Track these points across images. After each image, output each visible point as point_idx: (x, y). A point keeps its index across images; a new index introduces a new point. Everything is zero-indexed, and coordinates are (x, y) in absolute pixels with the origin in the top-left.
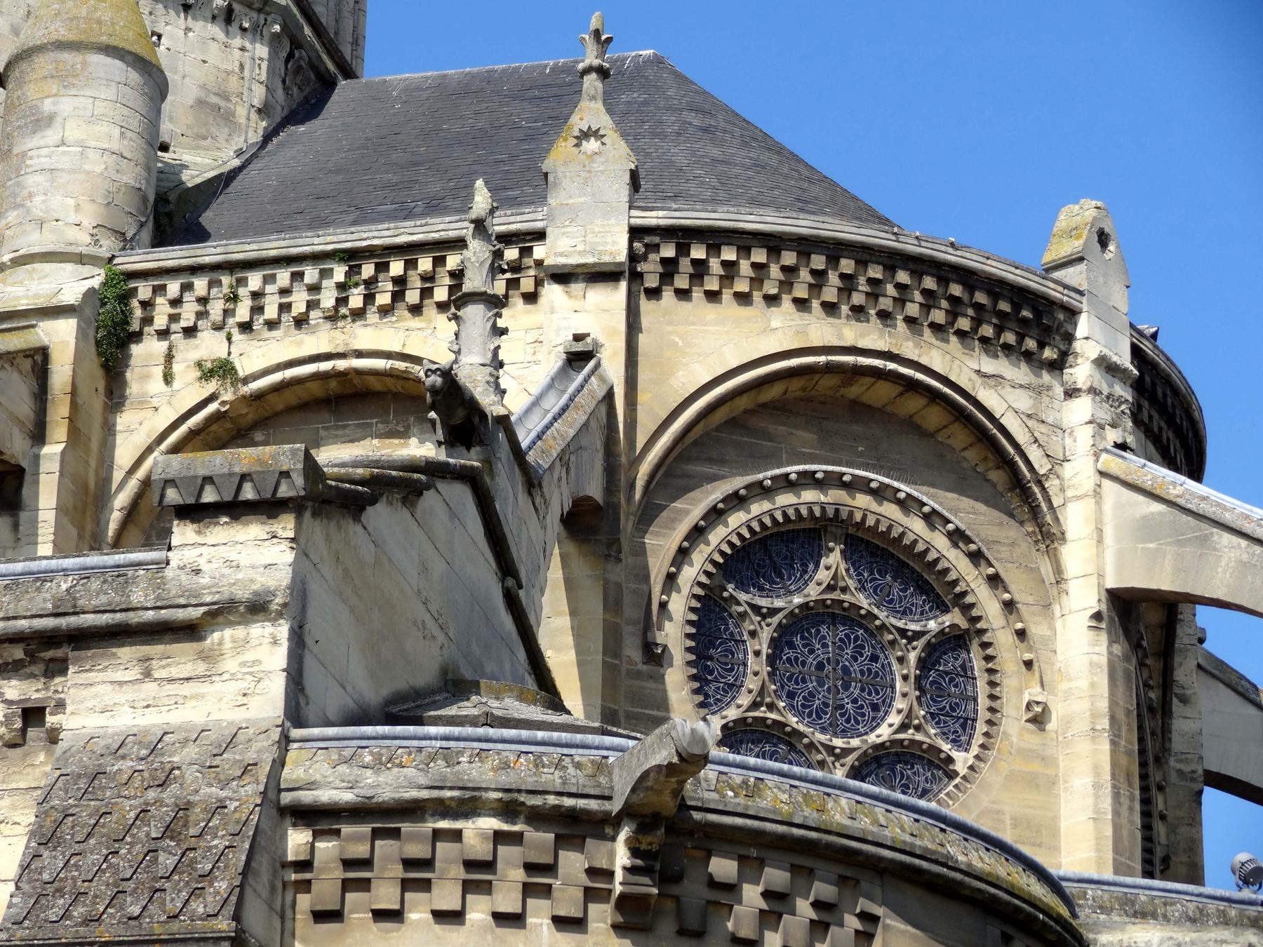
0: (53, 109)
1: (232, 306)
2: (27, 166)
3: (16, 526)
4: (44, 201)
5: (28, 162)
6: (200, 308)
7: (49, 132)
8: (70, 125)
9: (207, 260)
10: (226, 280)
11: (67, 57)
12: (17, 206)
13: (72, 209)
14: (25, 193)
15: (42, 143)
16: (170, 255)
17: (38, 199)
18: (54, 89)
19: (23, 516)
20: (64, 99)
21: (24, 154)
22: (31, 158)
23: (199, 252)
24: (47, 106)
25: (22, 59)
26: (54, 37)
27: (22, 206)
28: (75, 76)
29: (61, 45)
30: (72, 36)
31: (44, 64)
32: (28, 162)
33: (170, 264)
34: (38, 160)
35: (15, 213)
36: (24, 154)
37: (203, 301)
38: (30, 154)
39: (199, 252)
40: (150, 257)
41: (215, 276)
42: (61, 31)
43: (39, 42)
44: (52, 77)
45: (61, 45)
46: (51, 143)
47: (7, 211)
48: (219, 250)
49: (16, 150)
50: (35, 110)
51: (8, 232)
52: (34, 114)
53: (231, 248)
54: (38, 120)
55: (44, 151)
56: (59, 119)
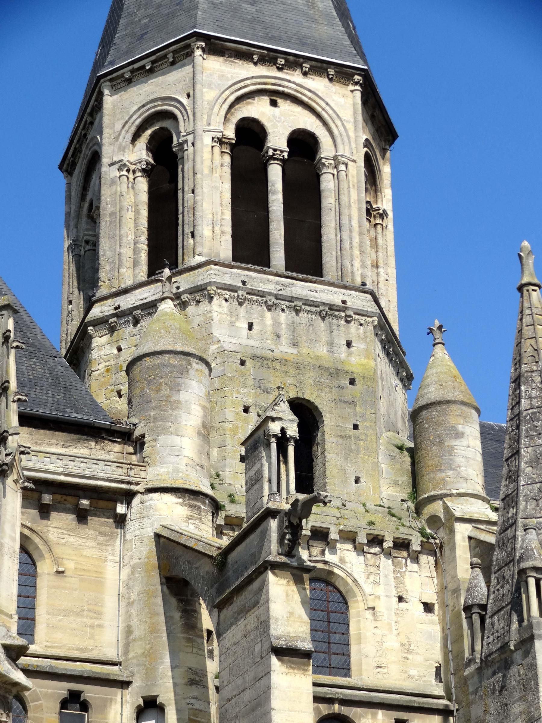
0: (463, 430)
2: (455, 453)
4: (466, 470)
5: (455, 451)
7: (462, 440)
8: (470, 439)
11: (464, 408)
12: (451, 469)
13: (476, 476)
15: (460, 444)
17: (463, 469)
18: (462, 422)
20: (466, 427)
21: (452, 447)
22: (456, 449)
24: (460, 428)
26: (460, 399)
27: (456, 470)
28: (469, 418)
29: (463, 403)
30: (465, 400)
31: (456, 409)
32: (455, 451)
34: (460, 451)
35: (451, 472)
36: (452, 447)
38: (456, 447)
42: (461, 397)
43: (453, 399)
45: (463, 403)
47: (445, 469)
49: (446, 444)
50: (454, 429)
52: (455, 431)
54: (457, 433)
55: (462, 448)
56: (466, 435)
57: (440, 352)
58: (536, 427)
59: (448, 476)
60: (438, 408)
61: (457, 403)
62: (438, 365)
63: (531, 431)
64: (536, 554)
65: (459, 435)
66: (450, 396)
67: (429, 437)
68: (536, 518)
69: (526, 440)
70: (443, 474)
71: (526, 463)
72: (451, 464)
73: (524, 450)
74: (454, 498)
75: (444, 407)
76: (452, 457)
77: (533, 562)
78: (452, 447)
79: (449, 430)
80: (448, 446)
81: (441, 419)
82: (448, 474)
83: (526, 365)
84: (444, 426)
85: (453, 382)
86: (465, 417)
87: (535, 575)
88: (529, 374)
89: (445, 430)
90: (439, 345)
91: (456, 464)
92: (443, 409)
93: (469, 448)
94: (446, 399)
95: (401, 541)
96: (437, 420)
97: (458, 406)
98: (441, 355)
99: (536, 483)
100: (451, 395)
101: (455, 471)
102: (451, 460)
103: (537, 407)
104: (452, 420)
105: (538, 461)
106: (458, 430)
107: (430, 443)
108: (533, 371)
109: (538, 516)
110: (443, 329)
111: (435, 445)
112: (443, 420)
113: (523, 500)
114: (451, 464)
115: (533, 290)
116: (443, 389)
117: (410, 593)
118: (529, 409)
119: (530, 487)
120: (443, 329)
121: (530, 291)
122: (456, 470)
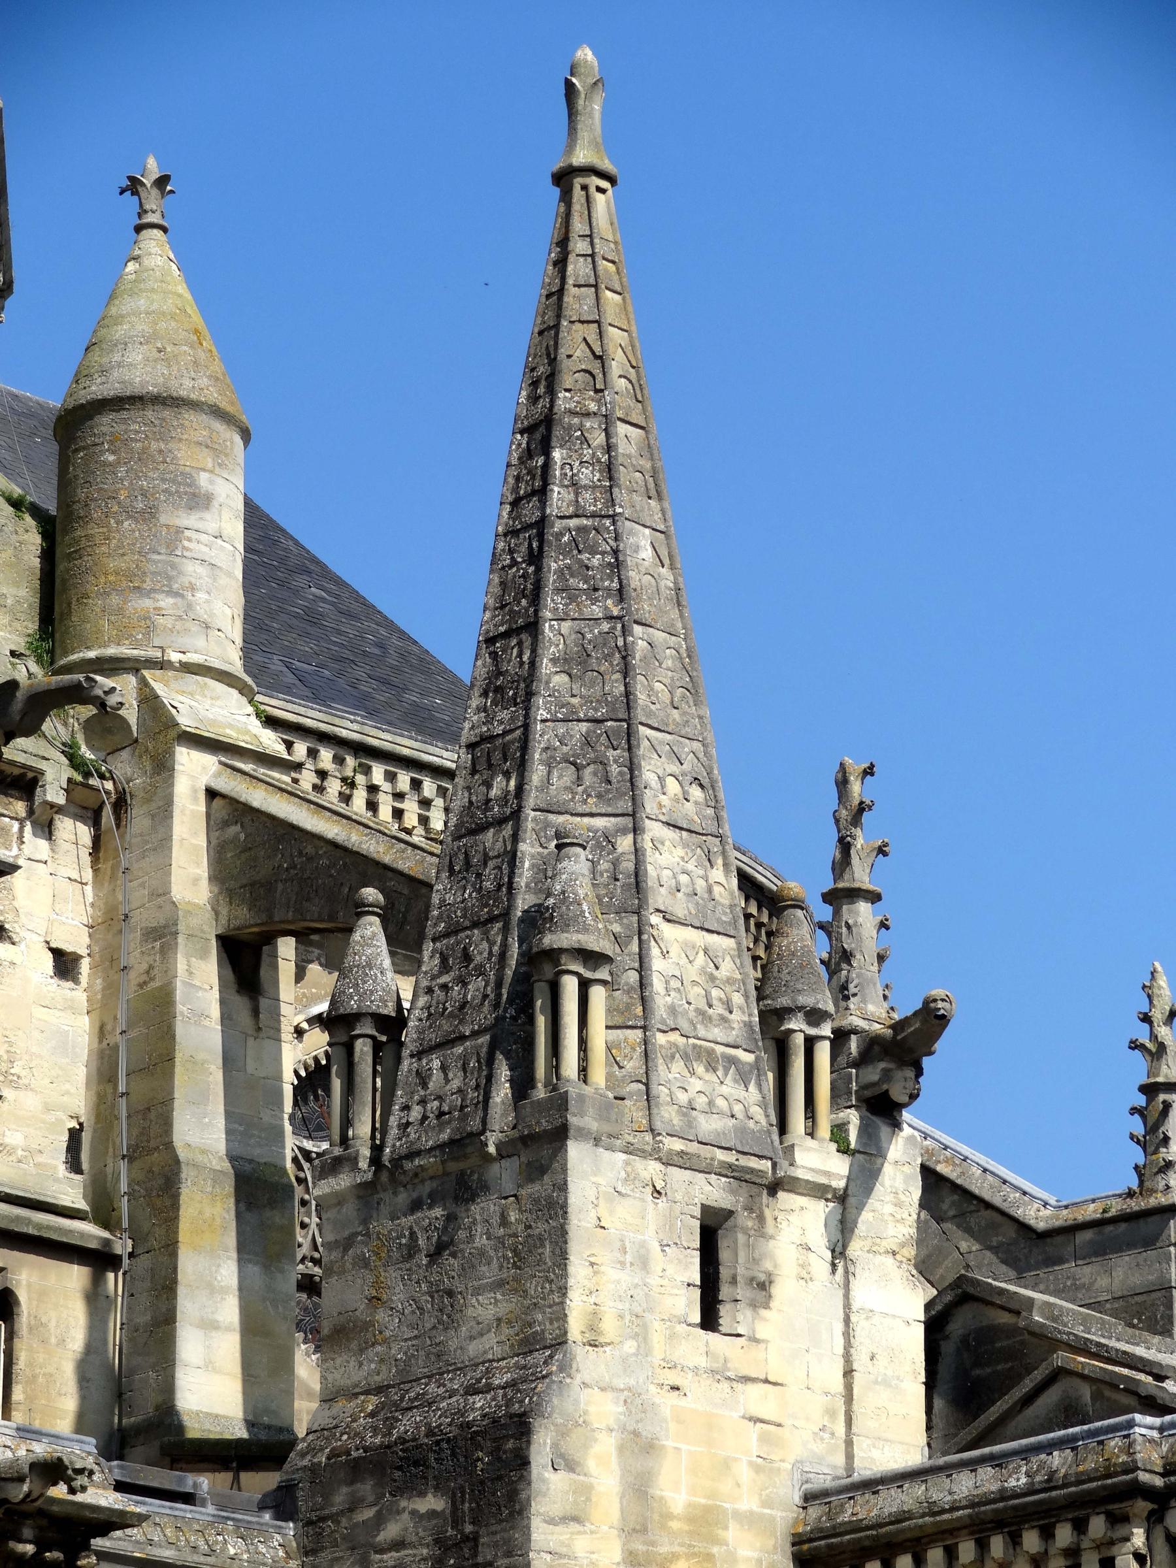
1: (348, 792)
2: (184, 548)
3: (256, 1012)
4: (207, 601)
5: (186, 543)
6: (318, 782)
7: (207, 515)
9: (344, 733)
10: (351, 761)
11: (219, 426)
14: (185, 580)
15: (199, 525)
16: (311, 713)
17: (201, 596)
19: (264, 1003)
20: (220, 481)
22: (189, 540)
23: (337, 721)
24: (203, 479)
25: (164, 404)
27: (182, 596)
28: (226, 455)
29: (217, 412)
31: (197, 425)
32: (186, 543)
33: (309, 723)
34: (197, 545)
36: (179, 531)
37: (322, 774)
38: (187, 533)
39: (337, 721)
40: (290, 706)
41: (341, 752)
42: (212, 395)
43: (193, 396)
44: (207, 447)
45: (217, 412)
46: (210, 532)
47: (153, 590)
48: (355, 727)
49: (163, 519)
50: (187, 480)
51: (161, 620)
52: (190, 485)
53: (367, 729)
54: (194, 495)
55: (204, 538)
56: (215, 503)
57: (156, 250)
58: (588, 568)
59: (159, 609)
60: (149, 414)
61: (202, 410)
62: (153, 290)
63: (572, 576)
64: (587, 915)
65: (200, 501)
66: (185, 387)
67: (117, 491)
68: (572, 815)
69: (558, 599)
70: (147, 603)
71: (554, 661)
72: (170, 579)
73: (551, 626)
74: (171, 673)
75: (167, 413)
76: (177, 560)
77: (580, 936)
78: (177, 532)
79: (174, 481)
80: (167, 526)
81: (154, 446)
82: (162, 604)
83: (567, 394)
84: (161, 467)
85: (192, 347)
86: (218, 451)
87: (581, 970)
88: (576, 420)
89: (164, 480)
90: (155, 231)
91: (185, 580)
92: (164, 419)
93: (219, 541)
94: (175, 394)
95: (17, 771)
96: (144, 450)
97: (204, 418)
98: (160, 261)
99: (579, 720)
100: (188, 383)
101: (179, 600)
102: (173, 566)
103: (594, 515)
104: (185, 456)
105: (585, 662)
106: (198, 487)
107: (116, 508)
108: (588, 414)
109: (580, 810)
110: (169, 188)
111: (131, 517)
112: (161, 451)
113: (541, 761)
114: (170, 579)
115: (601, 190)
116: (168, 362)
117: (23, 919)
118: (570, 517)
119: (561, 729)
120: (169, 188)
121: (592, 189)
122: (182, 596)
